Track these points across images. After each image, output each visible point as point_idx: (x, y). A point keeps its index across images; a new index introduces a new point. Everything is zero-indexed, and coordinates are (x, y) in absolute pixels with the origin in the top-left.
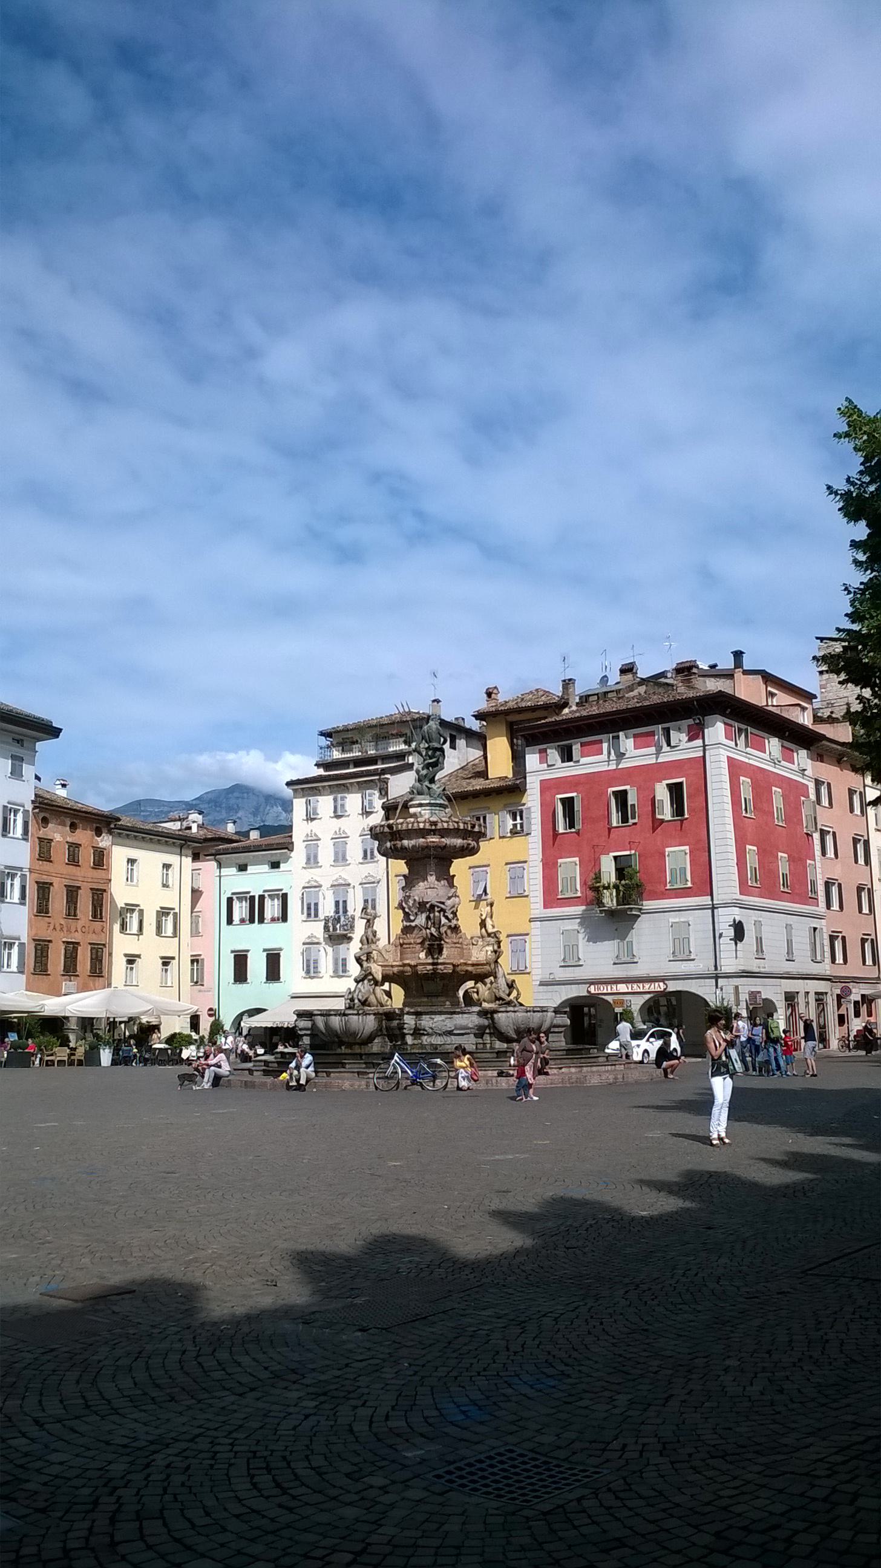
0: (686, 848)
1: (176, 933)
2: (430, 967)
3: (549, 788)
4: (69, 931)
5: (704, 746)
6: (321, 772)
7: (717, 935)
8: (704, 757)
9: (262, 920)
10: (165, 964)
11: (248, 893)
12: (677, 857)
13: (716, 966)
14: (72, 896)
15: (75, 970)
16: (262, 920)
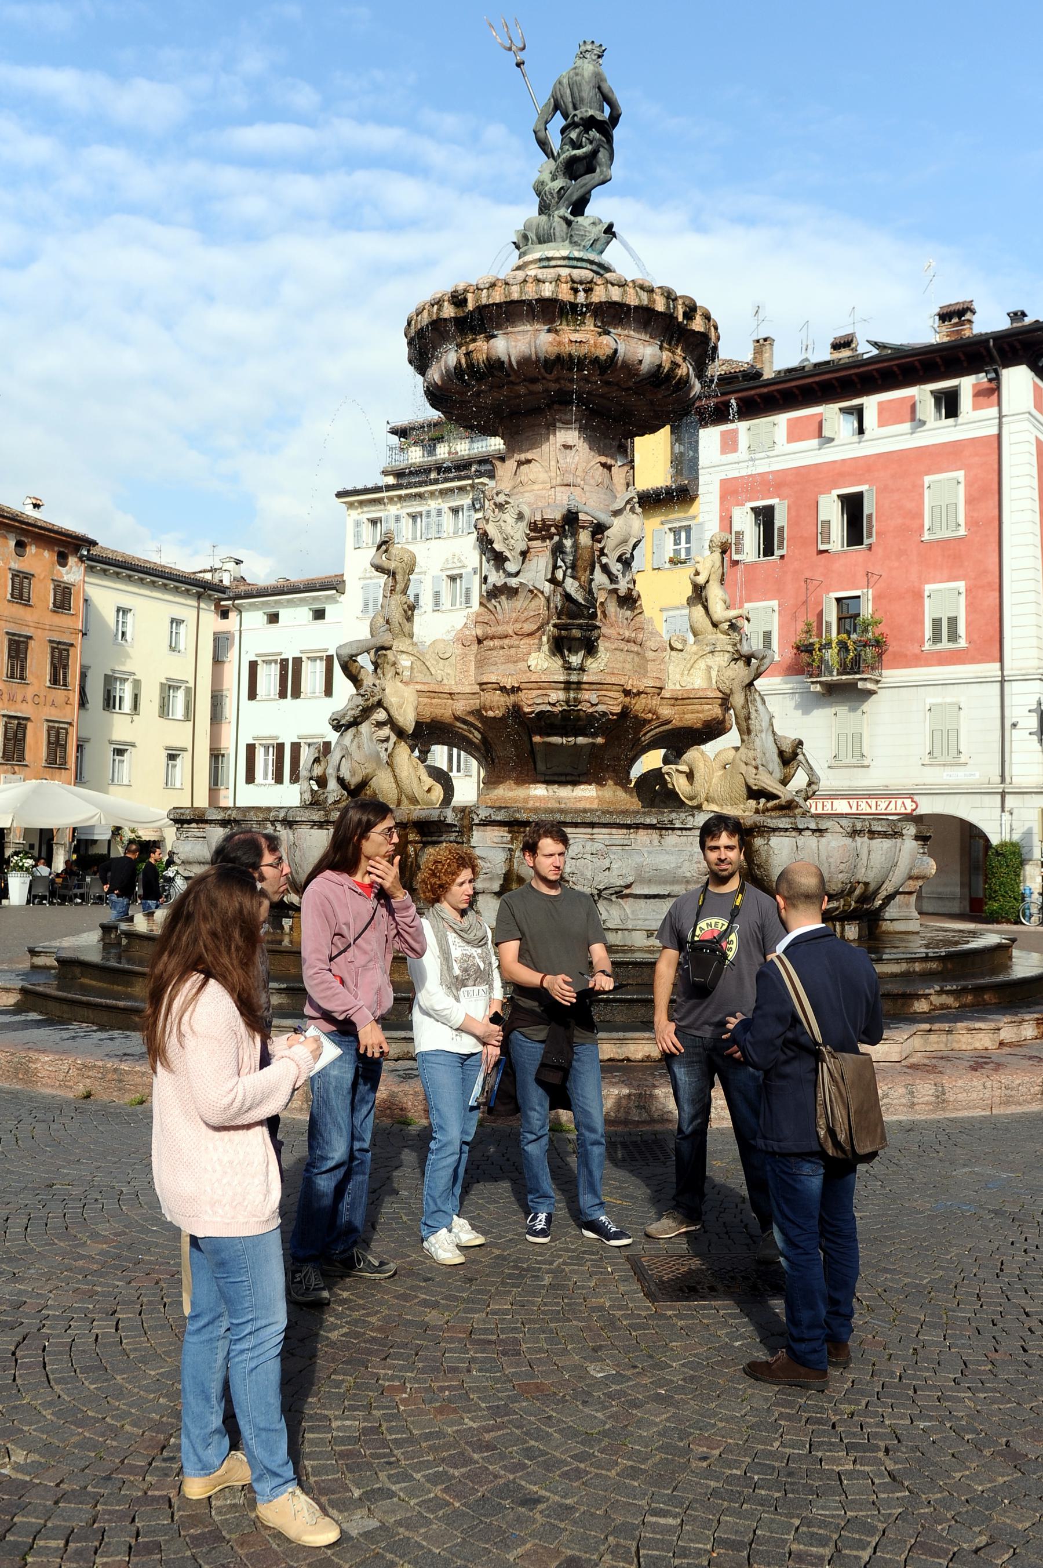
0: (961, 585)
1: (190, 713)
2: (557, 695)
3: (735, 492)
4: (12, 699)
5: (1000, 417)
6: (391, 480)
7: (1008, 725)
8: (999, 436)
9: (297, 694)
10: (172, 757)
11: (280, 654)
12: (945, 597)
13: (1003, 776)
14: (18, 651)
15: (22, 758)
16: (297, 694)
